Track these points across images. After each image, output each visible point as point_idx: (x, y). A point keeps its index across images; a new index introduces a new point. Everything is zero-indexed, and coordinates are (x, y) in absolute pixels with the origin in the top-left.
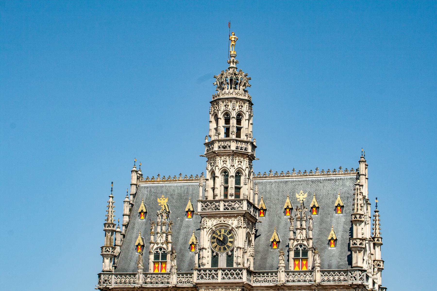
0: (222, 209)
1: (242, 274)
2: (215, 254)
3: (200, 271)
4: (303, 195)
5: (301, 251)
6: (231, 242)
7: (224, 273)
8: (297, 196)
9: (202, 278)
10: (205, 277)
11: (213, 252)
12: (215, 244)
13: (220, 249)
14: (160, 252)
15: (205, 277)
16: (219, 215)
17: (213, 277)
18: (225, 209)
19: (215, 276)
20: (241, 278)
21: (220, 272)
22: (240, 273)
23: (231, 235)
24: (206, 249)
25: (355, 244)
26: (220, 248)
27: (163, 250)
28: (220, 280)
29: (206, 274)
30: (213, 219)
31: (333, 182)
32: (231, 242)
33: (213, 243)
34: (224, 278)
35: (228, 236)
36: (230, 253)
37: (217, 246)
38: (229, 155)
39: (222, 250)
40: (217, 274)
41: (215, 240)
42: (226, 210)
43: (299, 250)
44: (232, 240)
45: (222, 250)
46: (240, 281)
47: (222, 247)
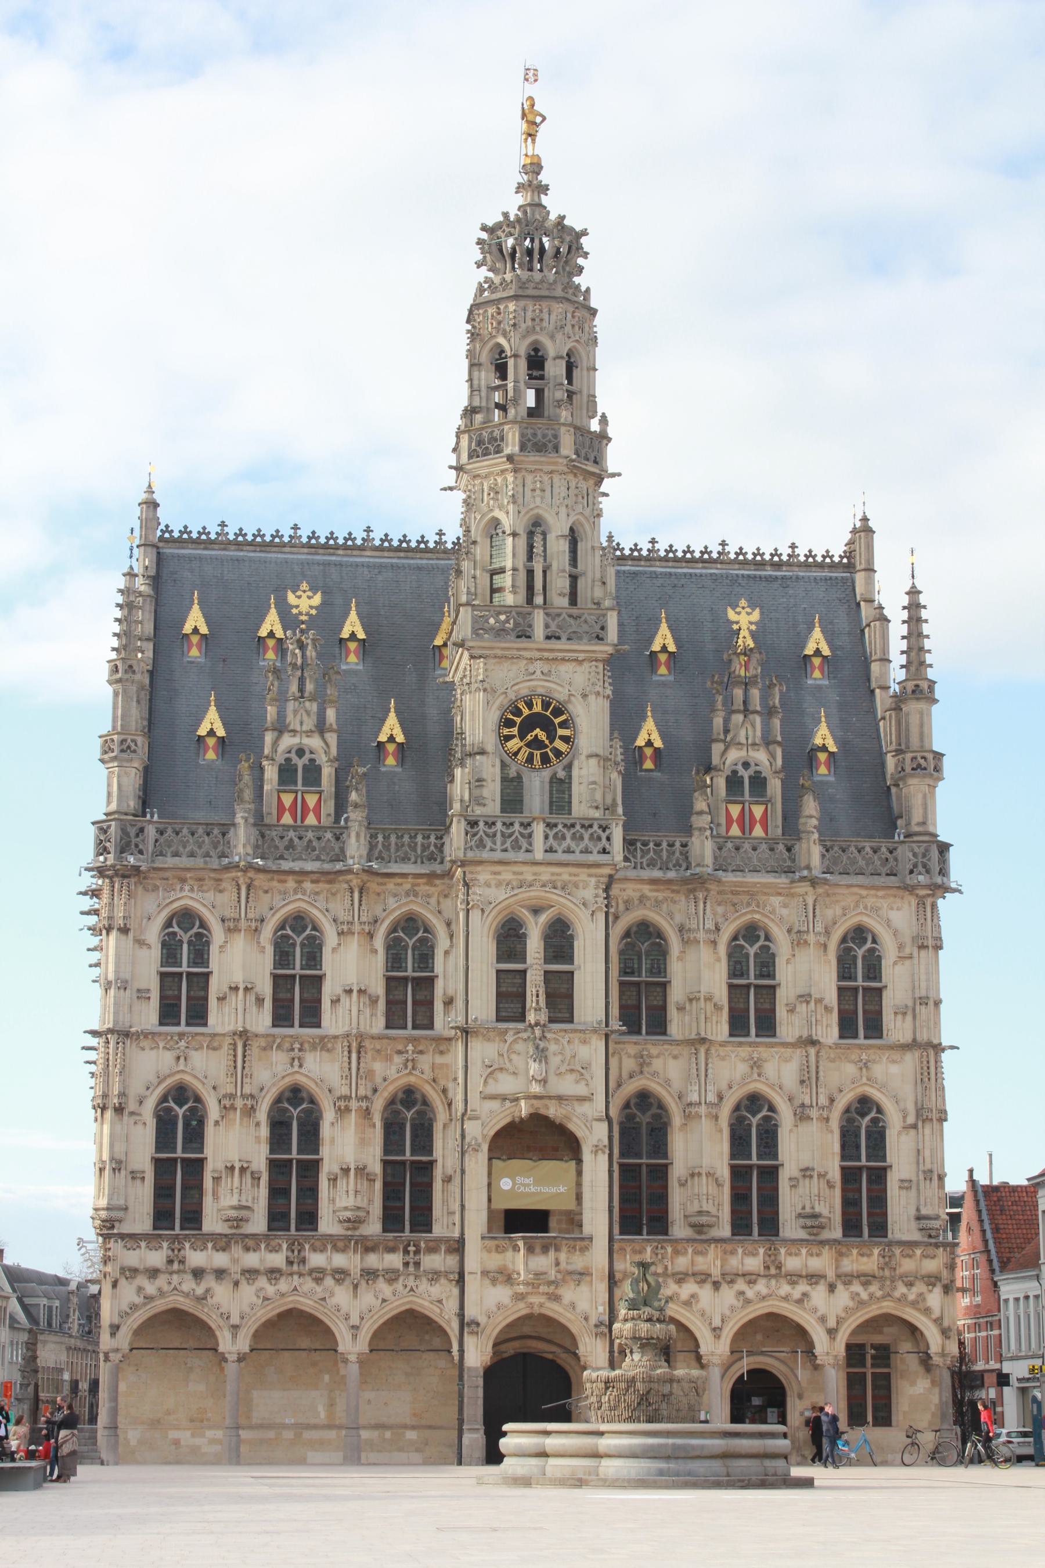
0: (539, 632)
3: (473, 824)
4: (748, 614)
6: (566, 739)
7: (551, 834)
8: (731, 615)
9: (481, 845)
13: (530, 759)
14: (300, 763)
15: (489, 844)
16: (527, 654)
17: (516, 846)
18: (548, 638)
20: (604, 851)
21: (539, 830)
22: (604, 836)
25: (919, 766)
26: (531, 755)
27: (308, 756)
29: (494, 835)
30: (506, 665)
31: (776, 585)
32: (566, 739)
34: (550, 850)
35: (557, 721)
36: (561, 774)
38: (551, 472)
40: (530, 835)
42: (553, 641)
43: (742, 777)
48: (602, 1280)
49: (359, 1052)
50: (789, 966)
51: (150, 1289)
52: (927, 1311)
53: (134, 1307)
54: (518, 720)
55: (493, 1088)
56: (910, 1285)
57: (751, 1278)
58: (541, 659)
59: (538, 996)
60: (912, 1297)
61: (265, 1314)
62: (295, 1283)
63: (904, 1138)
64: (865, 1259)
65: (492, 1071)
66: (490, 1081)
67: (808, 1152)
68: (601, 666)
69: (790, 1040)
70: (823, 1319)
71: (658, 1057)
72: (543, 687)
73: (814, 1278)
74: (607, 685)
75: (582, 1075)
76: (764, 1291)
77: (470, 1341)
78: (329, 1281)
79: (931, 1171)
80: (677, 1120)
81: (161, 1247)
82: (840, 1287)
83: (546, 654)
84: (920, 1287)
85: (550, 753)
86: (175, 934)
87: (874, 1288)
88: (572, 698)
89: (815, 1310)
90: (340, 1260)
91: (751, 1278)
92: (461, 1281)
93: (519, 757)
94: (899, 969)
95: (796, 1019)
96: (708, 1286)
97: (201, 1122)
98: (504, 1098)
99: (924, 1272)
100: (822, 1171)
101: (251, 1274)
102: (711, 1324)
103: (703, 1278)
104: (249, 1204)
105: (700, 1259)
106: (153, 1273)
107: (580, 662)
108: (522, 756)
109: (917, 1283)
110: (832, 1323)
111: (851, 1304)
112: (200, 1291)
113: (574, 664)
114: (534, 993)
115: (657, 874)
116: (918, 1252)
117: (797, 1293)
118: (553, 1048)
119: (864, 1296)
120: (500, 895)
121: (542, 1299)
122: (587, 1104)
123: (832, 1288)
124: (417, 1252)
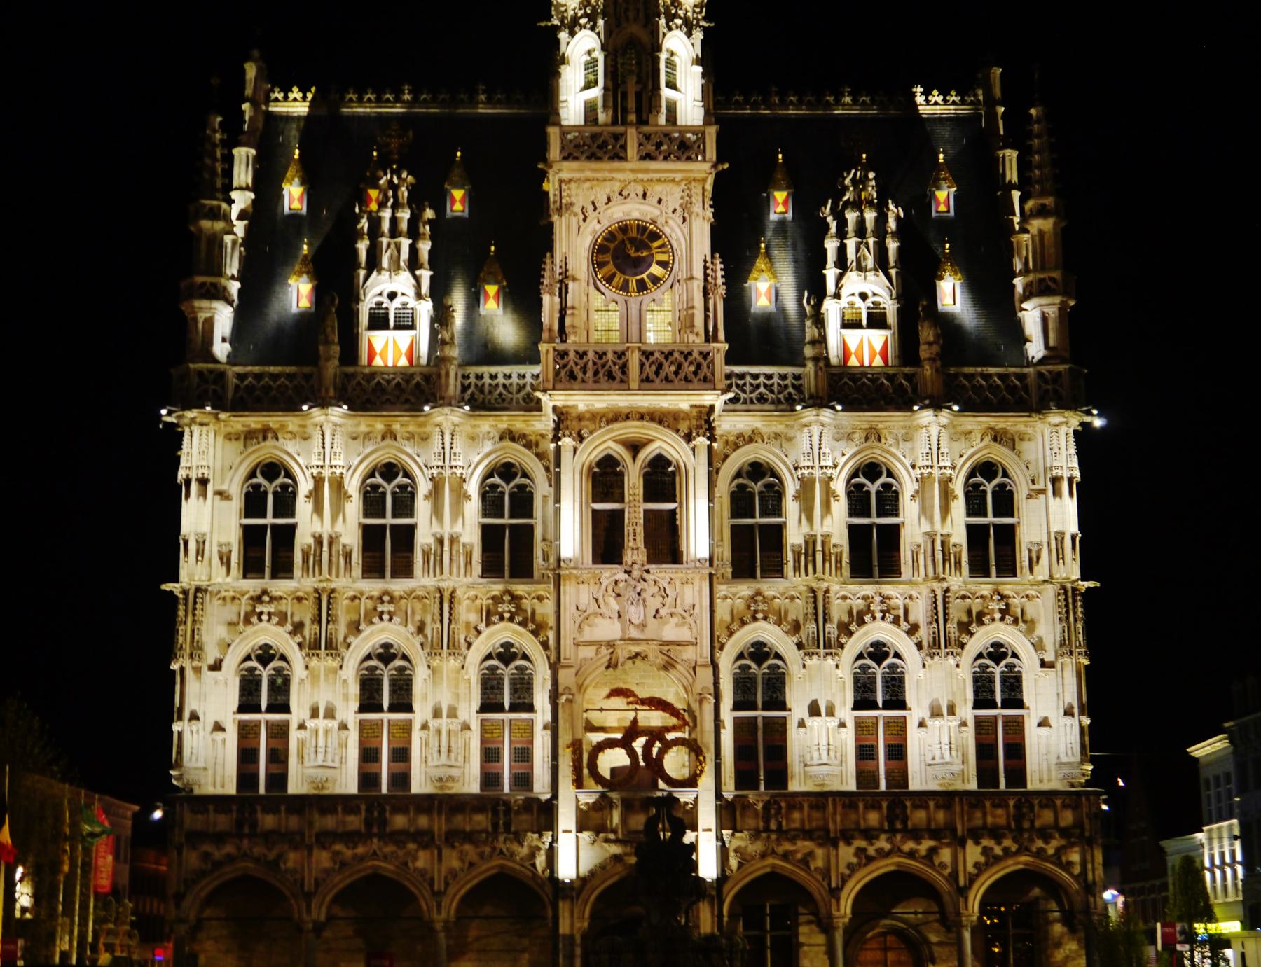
32: (664, 264)
33: (601, 265)
37: (614, 276)
44: (664, 258)
49: (451, 602)
51: (218, 855)
52: (1068, 866)
53: (202, 874)
54: (612, 246)
55: (588, 634)
56: (1047, 838)
61: (341, 881)
62: (375, 847)
74: (707, 206)
76: (887, 846)
81: (231, 811)
83: (640, 176)
86: (259, 485)
90: (423, 821)
97: (287, 681)
104: (336, 764)
106: (219, 838)
111: (982, 859)
112: (271, 856)
113: (671, 185)
116: (1058, 802)
119: (998, 851)
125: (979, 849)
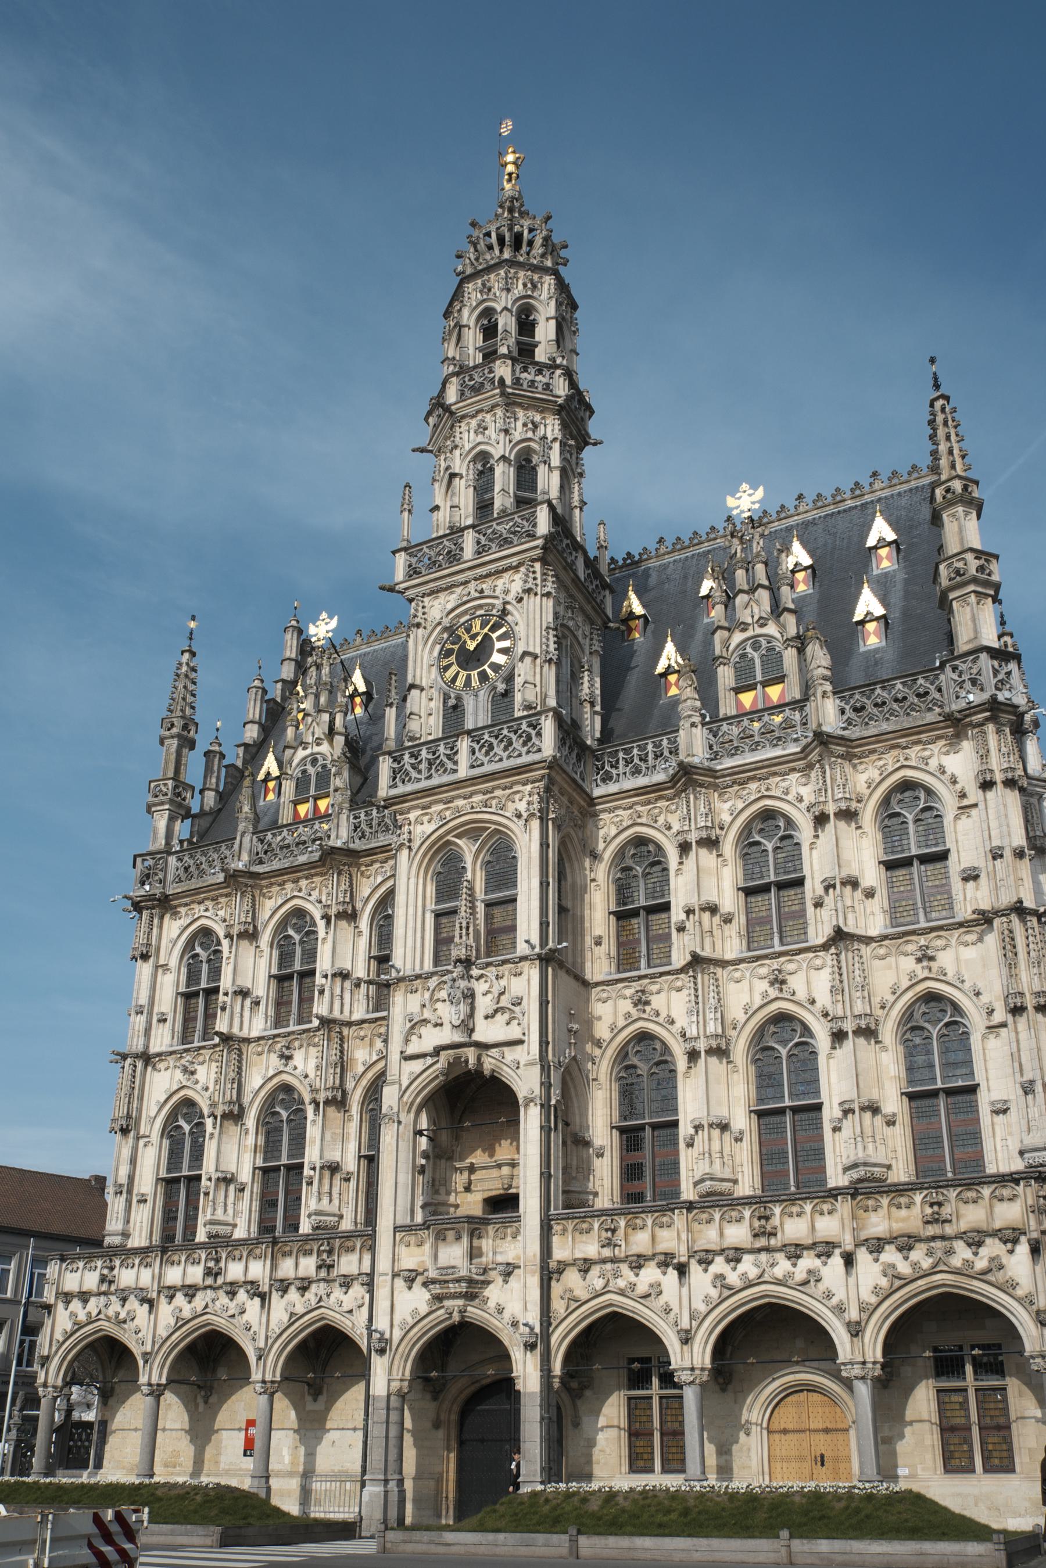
1: (539, 734)
2: (452, 702)
5: (758, 663)
10: (414, 774)
11: (446, 697)
12: (454, 668)
19: (450, 765)
21: (464, 745)
23: (504, 629)
24: (422, 689)
26: (469, 677)
28: (463, 772)
33: (446, 668)
35: (494, 636)
36: (501, 687)
39: (475, 682)
41: (453, 658)
45: (475, 682)
46: (537, 757)
47: (474, 674)
48: (533, 1273)
50: (814, 852)
57: (735, 1256)
58: (476, 579)
59: (468, 928)
60: (981, 1264)
63: (993, 1042)
64: (903, 1212)
65: (415, 1025)
66: (414, 1038)
67: (859, 1081)
68: (538, 566)
69: (821, 940)
70: (840, 1310)
71: (658, 992)
72: (480, 606)
73: (825, 1249)
75: (513, 1012)
76: (753, 1273)
77: (379, 1366)
78: (242, 1295)
79: (1032, 1082)
80: (681, 1063)
82: (863, 1256)
84: (993, 1248)
85: (489, 671)
87: (918, 1254)
88: (508, 607)
89: (829, 1295)
91: (735, 1256)
92: (370, 1286)
93: (457, 683)
94: (964, 823)
95: (825, 913)
96: (672, 1274)
98: (423, 1056)
99: (998, 1225)
100: (864, 1100)
101: (171, 1292)
102: (676, 1324)
103: (666, 1261)
105: (663, 1234)
107: (516, 568)
108: (460, 682)
109: (989, 1241)
110: (853, 1314)
111: (884, 1282)
114: (464, 925)
115: (641, 781)
117: (800, 1275)
118: (480, 987)
119: (904, 1268)
120: (428, 828)
121: (460, 1302)
122: (519, 1048)
123: (849, 1260)
124: (330, 1252)
125: (877, 1268)
